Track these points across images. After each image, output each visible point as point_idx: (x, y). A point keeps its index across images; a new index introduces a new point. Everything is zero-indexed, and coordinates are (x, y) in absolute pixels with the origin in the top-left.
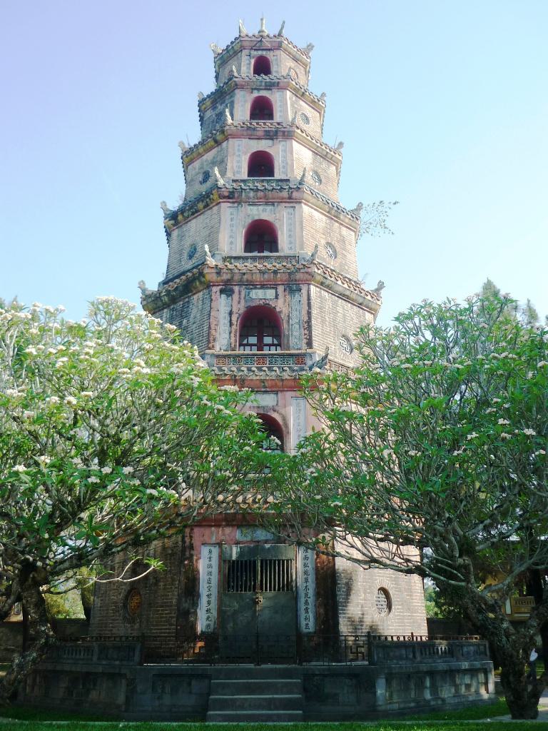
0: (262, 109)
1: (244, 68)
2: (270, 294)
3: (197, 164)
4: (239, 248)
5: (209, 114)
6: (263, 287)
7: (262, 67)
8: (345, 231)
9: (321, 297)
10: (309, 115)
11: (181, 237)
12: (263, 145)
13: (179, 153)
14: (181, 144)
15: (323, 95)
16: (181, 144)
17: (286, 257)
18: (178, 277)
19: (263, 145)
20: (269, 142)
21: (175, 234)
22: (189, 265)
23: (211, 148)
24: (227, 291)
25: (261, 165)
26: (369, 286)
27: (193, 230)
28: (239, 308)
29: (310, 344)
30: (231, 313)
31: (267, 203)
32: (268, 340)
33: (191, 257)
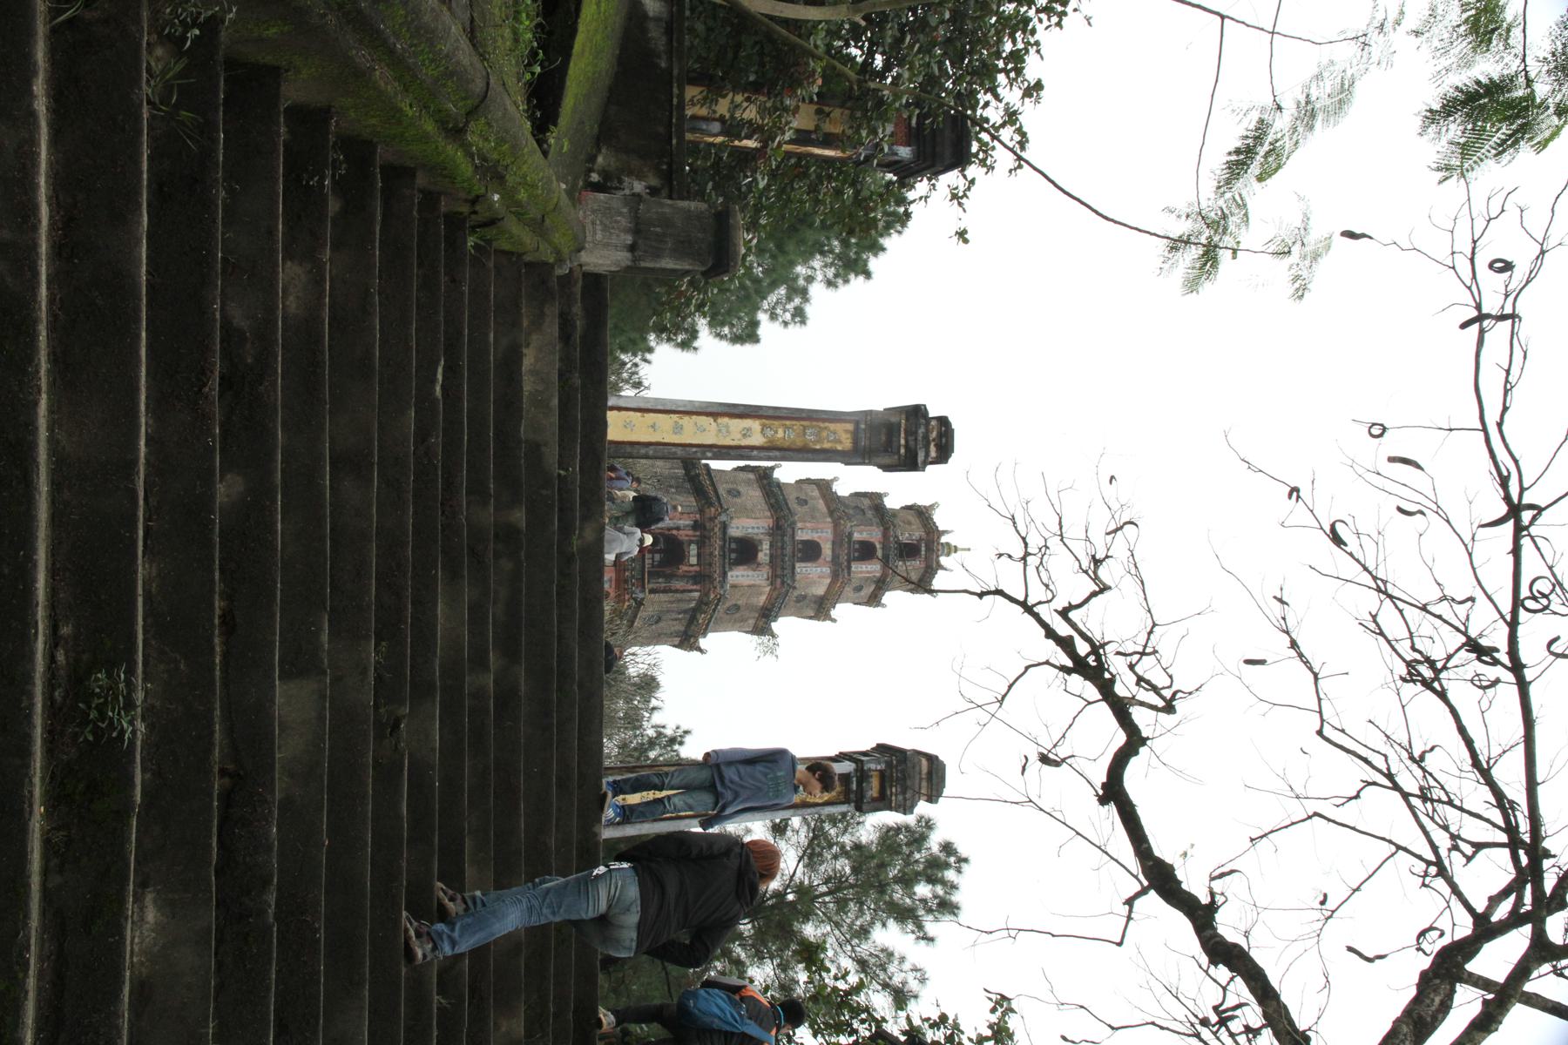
0: (866, 551)
1: (910, 533)
2: (693, 560)
3: (816, 493)
4: (734, 531)
5: (867, 502)
6: (699, 556)
7: (909, 551)
8: (752, 622)
9: (690, 601)
10: (862, 593)
11: (748, 482)
12: (827, 550)
13: (828, 477)
14: (836, 479)
15: (884, 606)
16: (836, 479)
17: (724, 575)
18: (713, 484)
19: (827, 550)
20: (829, 559)
21: (751, 476)
22: (722, 491)
23: (828, 508)
24: (696, 526)
25: (811, 551)
26: (703, 642)
27: (752, 493)
28: (683, 535)
29: (652, 591)
30: (678, 529)
31: (771, 556)
32: (657, 557)
33: (729, 492)
